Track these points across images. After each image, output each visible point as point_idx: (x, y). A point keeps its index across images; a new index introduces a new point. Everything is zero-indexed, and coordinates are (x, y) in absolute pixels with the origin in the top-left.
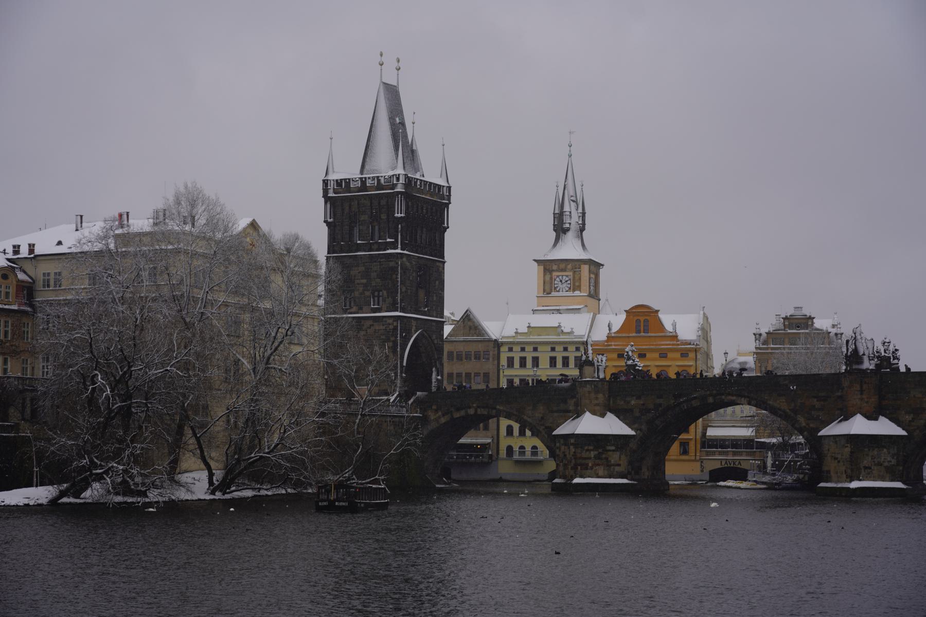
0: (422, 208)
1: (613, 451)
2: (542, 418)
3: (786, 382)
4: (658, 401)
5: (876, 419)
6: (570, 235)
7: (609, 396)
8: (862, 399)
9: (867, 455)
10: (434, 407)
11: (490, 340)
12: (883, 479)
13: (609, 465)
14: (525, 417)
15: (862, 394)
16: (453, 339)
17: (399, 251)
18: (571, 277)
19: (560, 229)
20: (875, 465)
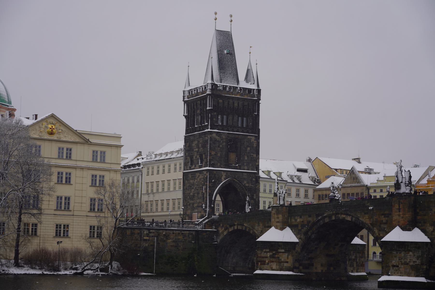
0: (234, 103)
1: (283, 252)
2: (262, 231)
4: (310, 219)
5: (410, 230)
8: (399, 215)
9: (396, 257)
10: (221, 225)
11: (364, 186)
12: (409, 275)
13: (279, 262)
14: (255, 231)
15: (399, 212)
16: (345, 185)
17: (209, 130)
20: (402, 264)
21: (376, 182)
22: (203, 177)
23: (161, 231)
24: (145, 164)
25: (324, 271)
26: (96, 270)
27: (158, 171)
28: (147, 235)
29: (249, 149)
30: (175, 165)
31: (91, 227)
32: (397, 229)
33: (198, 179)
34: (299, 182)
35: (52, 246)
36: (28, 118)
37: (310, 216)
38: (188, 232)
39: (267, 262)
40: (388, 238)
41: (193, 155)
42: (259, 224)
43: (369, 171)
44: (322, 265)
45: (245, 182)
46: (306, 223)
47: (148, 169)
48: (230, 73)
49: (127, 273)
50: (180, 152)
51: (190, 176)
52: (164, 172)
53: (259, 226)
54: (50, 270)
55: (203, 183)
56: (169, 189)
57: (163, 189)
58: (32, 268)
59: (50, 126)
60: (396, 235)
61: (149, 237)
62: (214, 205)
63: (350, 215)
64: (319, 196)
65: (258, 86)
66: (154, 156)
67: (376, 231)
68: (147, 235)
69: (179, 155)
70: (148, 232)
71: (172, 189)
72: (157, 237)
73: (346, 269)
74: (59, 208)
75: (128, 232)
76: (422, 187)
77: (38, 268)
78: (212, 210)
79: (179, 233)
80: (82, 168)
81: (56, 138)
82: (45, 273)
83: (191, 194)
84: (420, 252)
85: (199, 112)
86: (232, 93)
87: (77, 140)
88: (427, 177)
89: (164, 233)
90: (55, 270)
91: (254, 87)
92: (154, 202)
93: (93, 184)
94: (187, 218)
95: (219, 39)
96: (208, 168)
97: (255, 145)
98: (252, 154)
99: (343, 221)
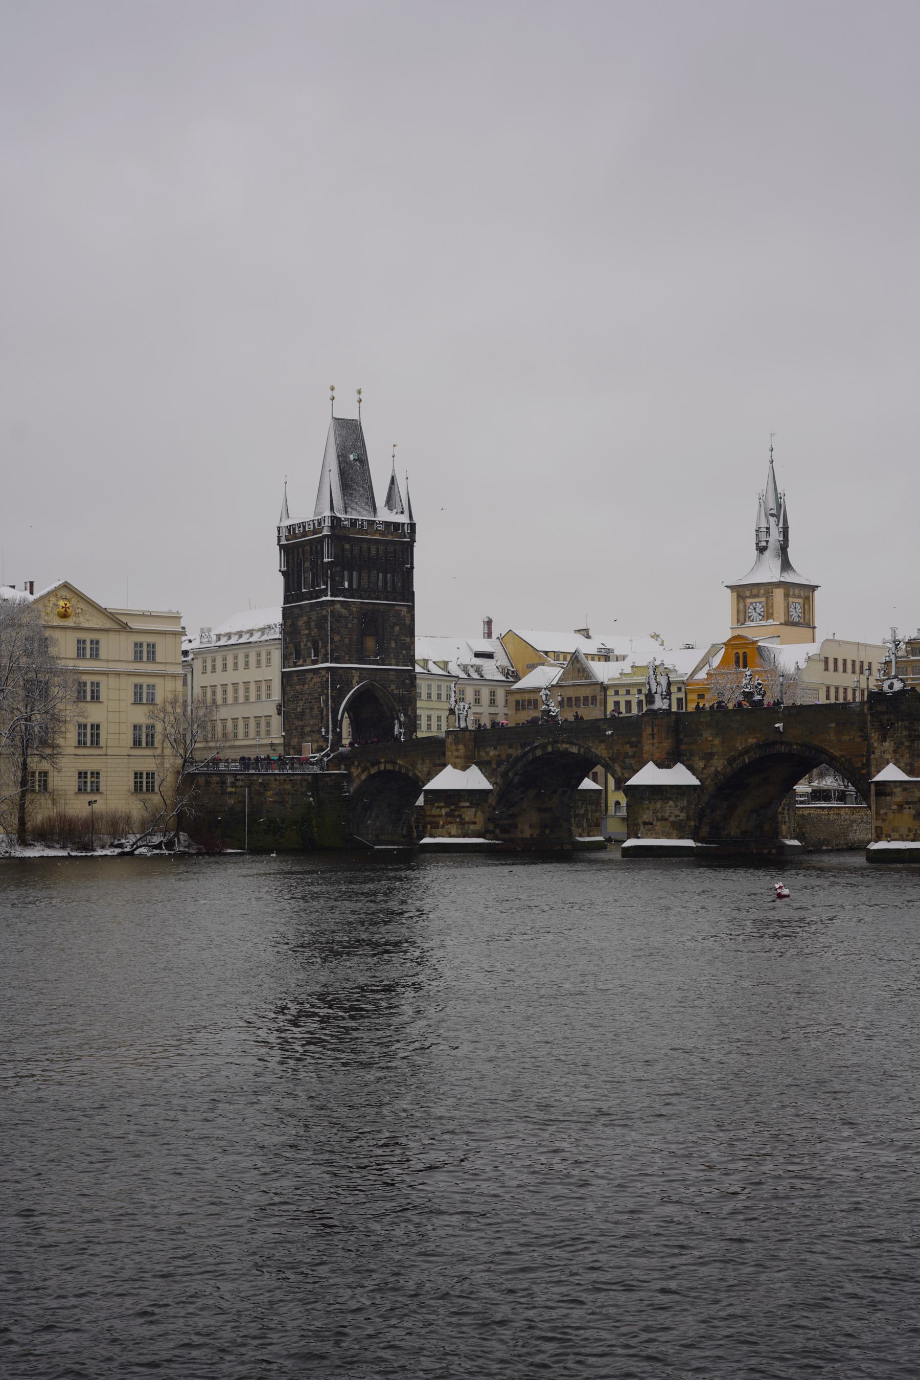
0: (369, 549)
1: (468, 807)
2: (429, 772)
3: (606, 726)
4: (511, 751)
5: (669, 767)
6: (767, 553)
7: (475, 747)
8: (653, 744)
9: (648, 809)
10: (356, 763)
11: (597, 684)
12: (668, 836)
13: (463, 823)
16: (564, 683)
17: (329, 598)
18: (764, 604)
19: (761, 550)
20: (658, 820)
21: (619, 676)
22: (319, 680)
23: (255, 778)
24: (198, 653)
25: (535, 836)
26: (158, 846)
27: (225, 666)
28: (233, 785)
29: (397, 628)
30: (259, 655)
31: (136, 774)
32: (650, 766)
33: (311, 684)
34: (478, 677)
35: (78, 807)
36: (13, 587)
37: (510, 747)
38: (300, 777)
39: (441, 823)
40: (637, 779)
41: (300, 642)
42: (423, 760)
43: (605, 656)
44: (531, 827)
45: (393, 687)
46: (504, 757)
47: (205, 661)
48: (361, 496)
49: (204, 850)
50: (267, 631)
51: (295, 678)
52: (236, 667)
53: (423, 763)
54: (77, 850)
55: (319, 690)
56: (247, 698)
57: (236, 699)
58: (49, 847)
59: (62, 603)
60: (649, 775)
61: (236, 787)
62: (341, 728)
63: (576, 744)
64: (517, 702)
65: (411, 517)
66: (214, 638)
67: (618, 769)
68: (233, 785)
69: (265, 638)
70: (233, 780)
71: (253, 698)
72: (249, 787)
73: (570, 831)
74: (81, 744)
75: (202, 780)
76: (698, 684)
77: (58, 846)
78: (338, 736)
79: (285, 780)
80: (118, 674)
81: (72, 624)
82: (73, 854)
83: (298, 710)
84: (685, 801)
85: (307, 564)
86: (366, 532)
87: (108, 624)
88: (707, 667)
89: (260, 781)
90: (87, 850)
91: (403, 519)
92: (219, 722)
93: (138, 701)
94: (292, 751)
95: (340, 435)
96: (328, 665)
97: (408, 622)
98: (403, 638)
99: (567, 754)
